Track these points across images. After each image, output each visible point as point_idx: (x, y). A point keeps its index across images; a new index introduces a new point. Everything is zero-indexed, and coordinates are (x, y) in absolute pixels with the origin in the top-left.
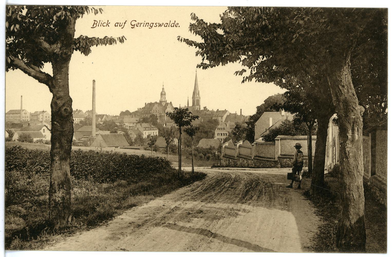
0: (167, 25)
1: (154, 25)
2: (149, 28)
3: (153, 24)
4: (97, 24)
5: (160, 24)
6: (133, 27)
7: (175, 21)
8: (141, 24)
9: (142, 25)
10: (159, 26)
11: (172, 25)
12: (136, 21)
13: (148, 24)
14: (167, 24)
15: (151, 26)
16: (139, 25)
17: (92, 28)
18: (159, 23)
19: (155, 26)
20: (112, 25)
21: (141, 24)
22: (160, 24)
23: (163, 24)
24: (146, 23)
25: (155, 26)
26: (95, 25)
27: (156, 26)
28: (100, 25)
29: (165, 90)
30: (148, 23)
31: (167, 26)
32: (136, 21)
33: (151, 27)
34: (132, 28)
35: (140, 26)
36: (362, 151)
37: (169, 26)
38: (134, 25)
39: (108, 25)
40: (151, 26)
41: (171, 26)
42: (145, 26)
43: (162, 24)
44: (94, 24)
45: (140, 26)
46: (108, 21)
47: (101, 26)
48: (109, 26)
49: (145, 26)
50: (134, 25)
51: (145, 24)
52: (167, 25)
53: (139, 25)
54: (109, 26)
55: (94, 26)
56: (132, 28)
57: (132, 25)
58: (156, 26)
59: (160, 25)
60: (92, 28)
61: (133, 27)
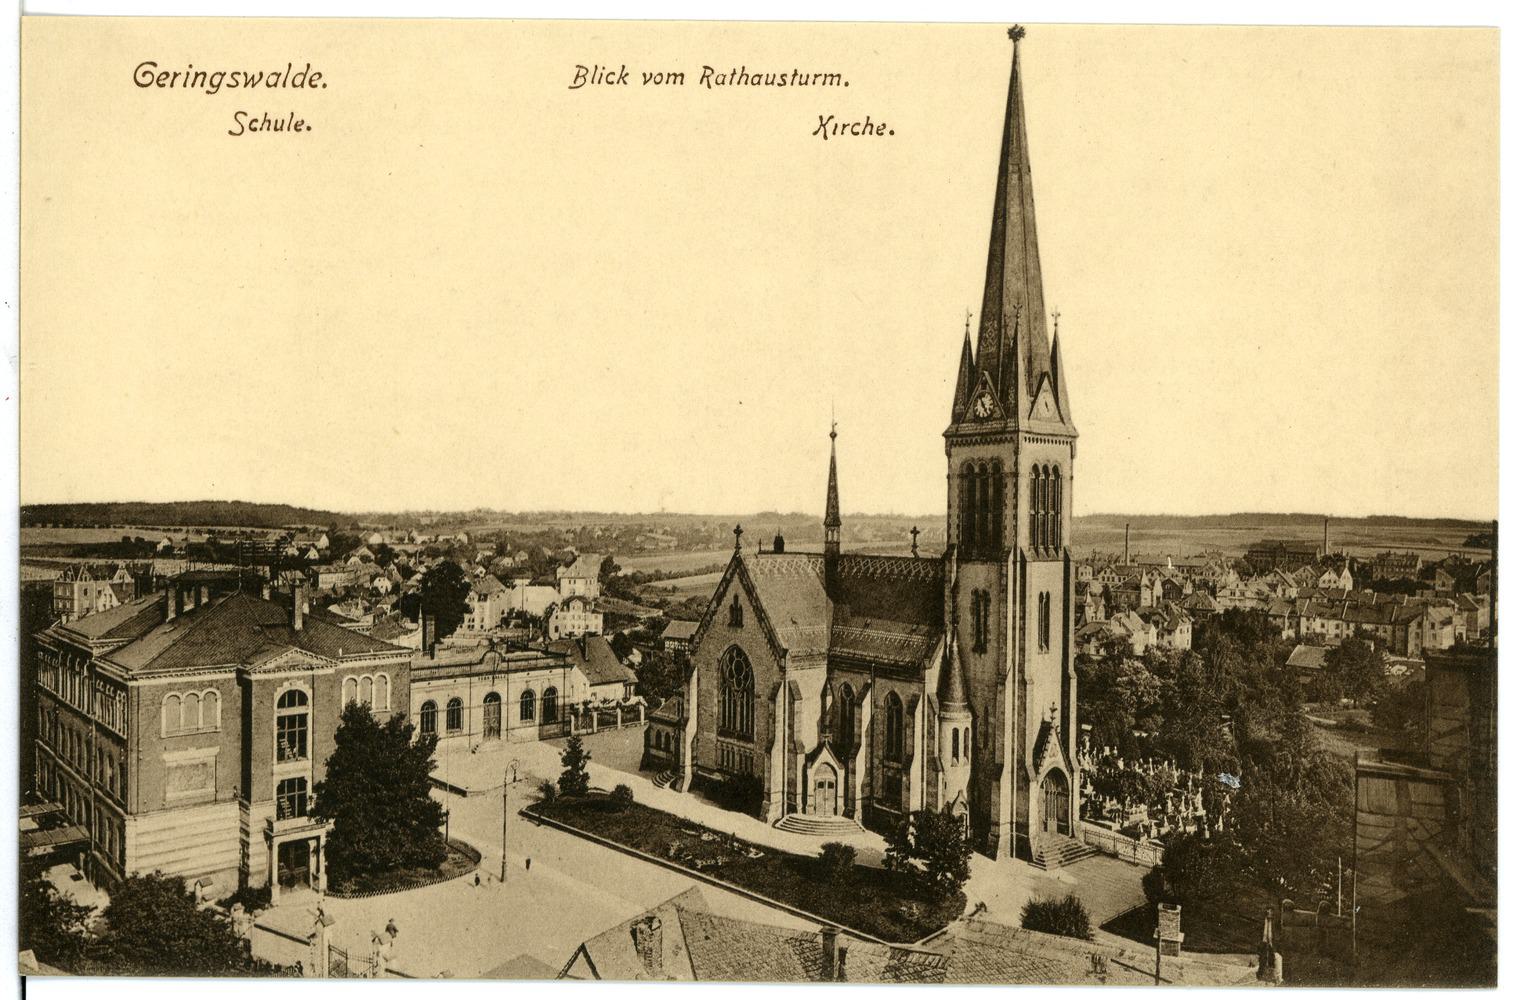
1: (227, 80)
3: (223, 75)
4: (589, 77)
15: (215, 82)
17: (571, 88)
19: (229, 85)
20: (635, 79)
25: (229, 85)
26: (580, 81)
27: (234, 83)
28: (596, 81)
39: (623, 78)
40: (215, 82)
44: (578, 76)
46: (624, 67)
47: (599, 82)
48: (625, 83)
51: (192, 76)
54: (625, 83)
55: (578, 84)
58: (233, 83)
60: (571, 88)
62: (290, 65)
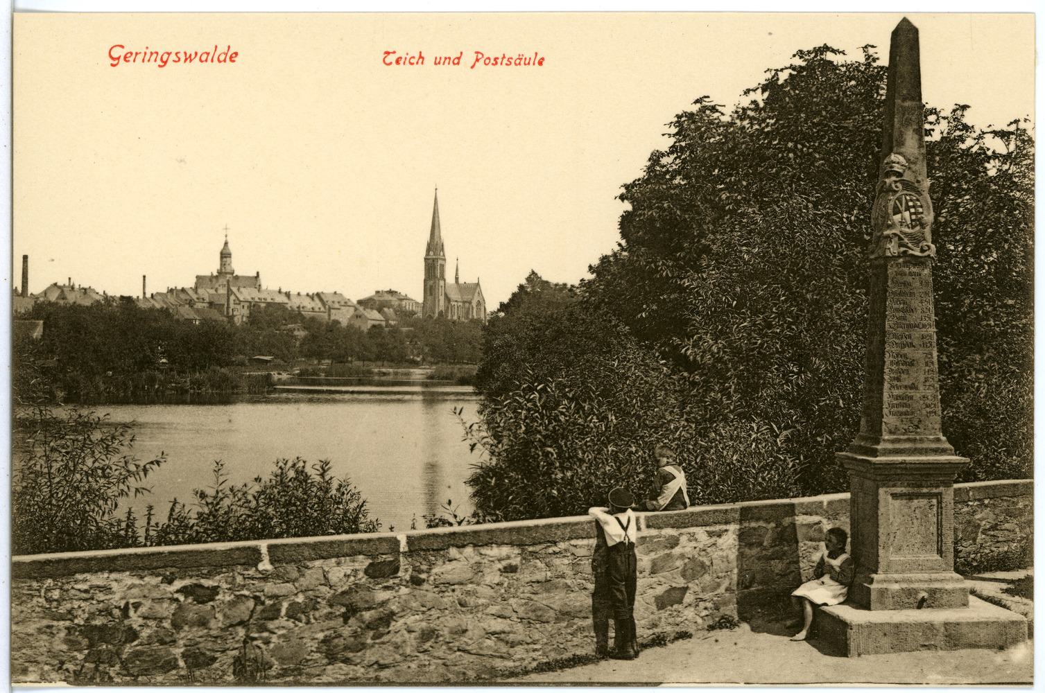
0: (205, 58)
1: (173, 57)
2: (159, 66)
3: (169, 54)
5: (188, 56)
6: (115, 62)
7: (229, 47)
8: (137, 54)
9: (140, 57)
10: (186, 60)
11: (222, 58)
12: (122, 47)
13: (155, 55)
14: (208, 54)
15: (164, 59)
16: (132, 59)
18: (185, 53)
19: (174, 61)
21: (137, 54)
22: (188, 56)
23: (196, 54)
24: (152, 53)
25: (174, 61)
27: (177, 59)
29: (231, 247)
30: (157, 53)
31: (206, 61)
32: (122, 47)
33: (162, 64)
34: (113, 65)
35: (134, 61)
36: (795, 501)
37: (212, 61)
38: (119, 58)
40: (164, 59)
41: (219, 61)
42: (149, 61)
43: (193, 57)
45: (134, 61)
49: (149, 61)
50: (119, 58)
52: (205, 58)
53: (132, 59)
56: (113, 65)
57: (111, 57)
58: (177, 59)
59: (188, 58)
61: (115, 62)
62: (216, 47)
